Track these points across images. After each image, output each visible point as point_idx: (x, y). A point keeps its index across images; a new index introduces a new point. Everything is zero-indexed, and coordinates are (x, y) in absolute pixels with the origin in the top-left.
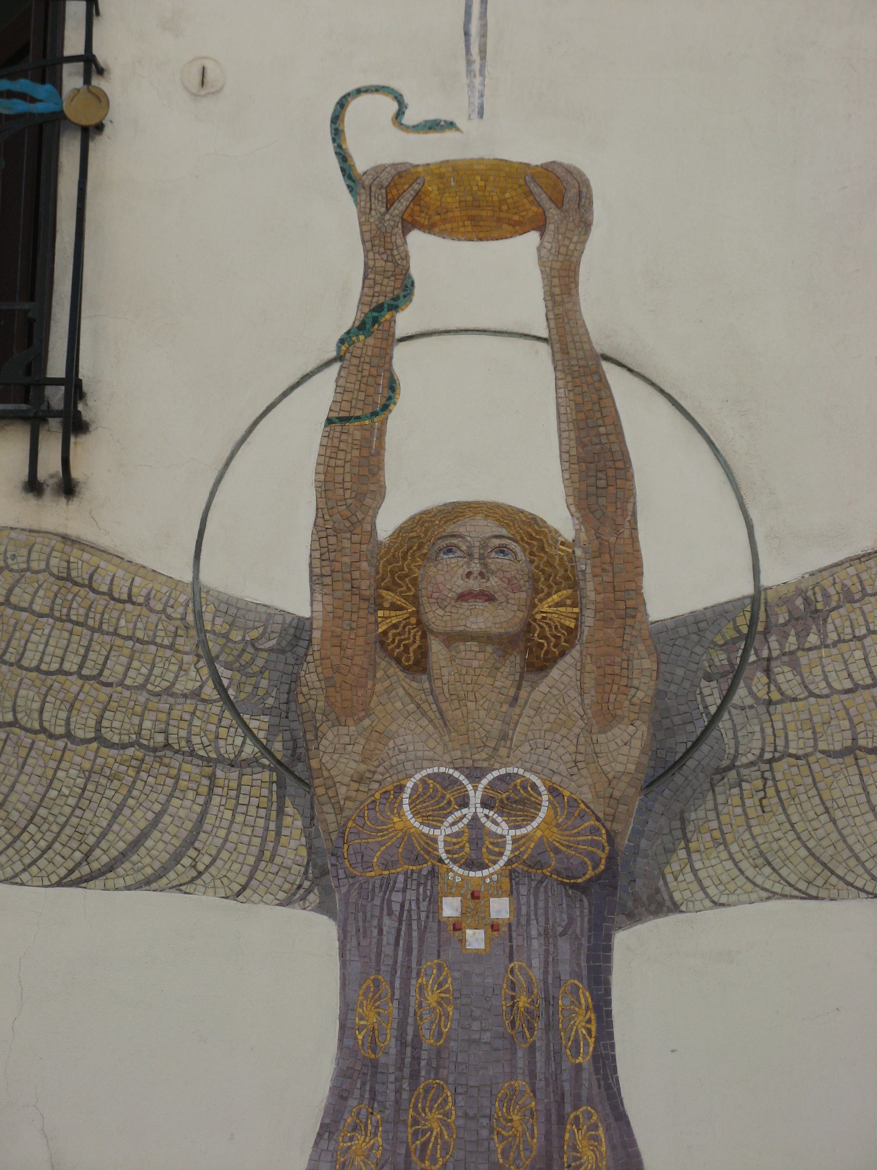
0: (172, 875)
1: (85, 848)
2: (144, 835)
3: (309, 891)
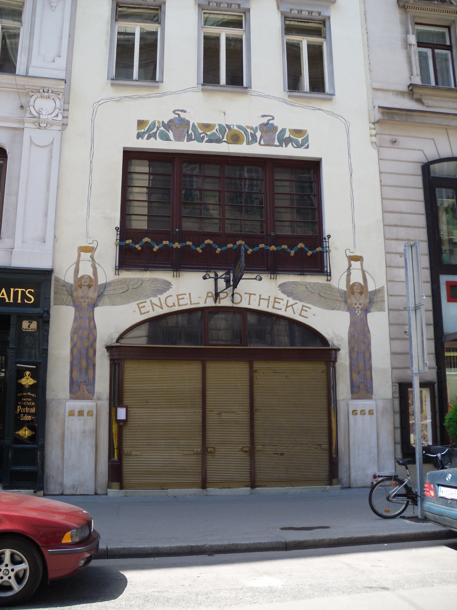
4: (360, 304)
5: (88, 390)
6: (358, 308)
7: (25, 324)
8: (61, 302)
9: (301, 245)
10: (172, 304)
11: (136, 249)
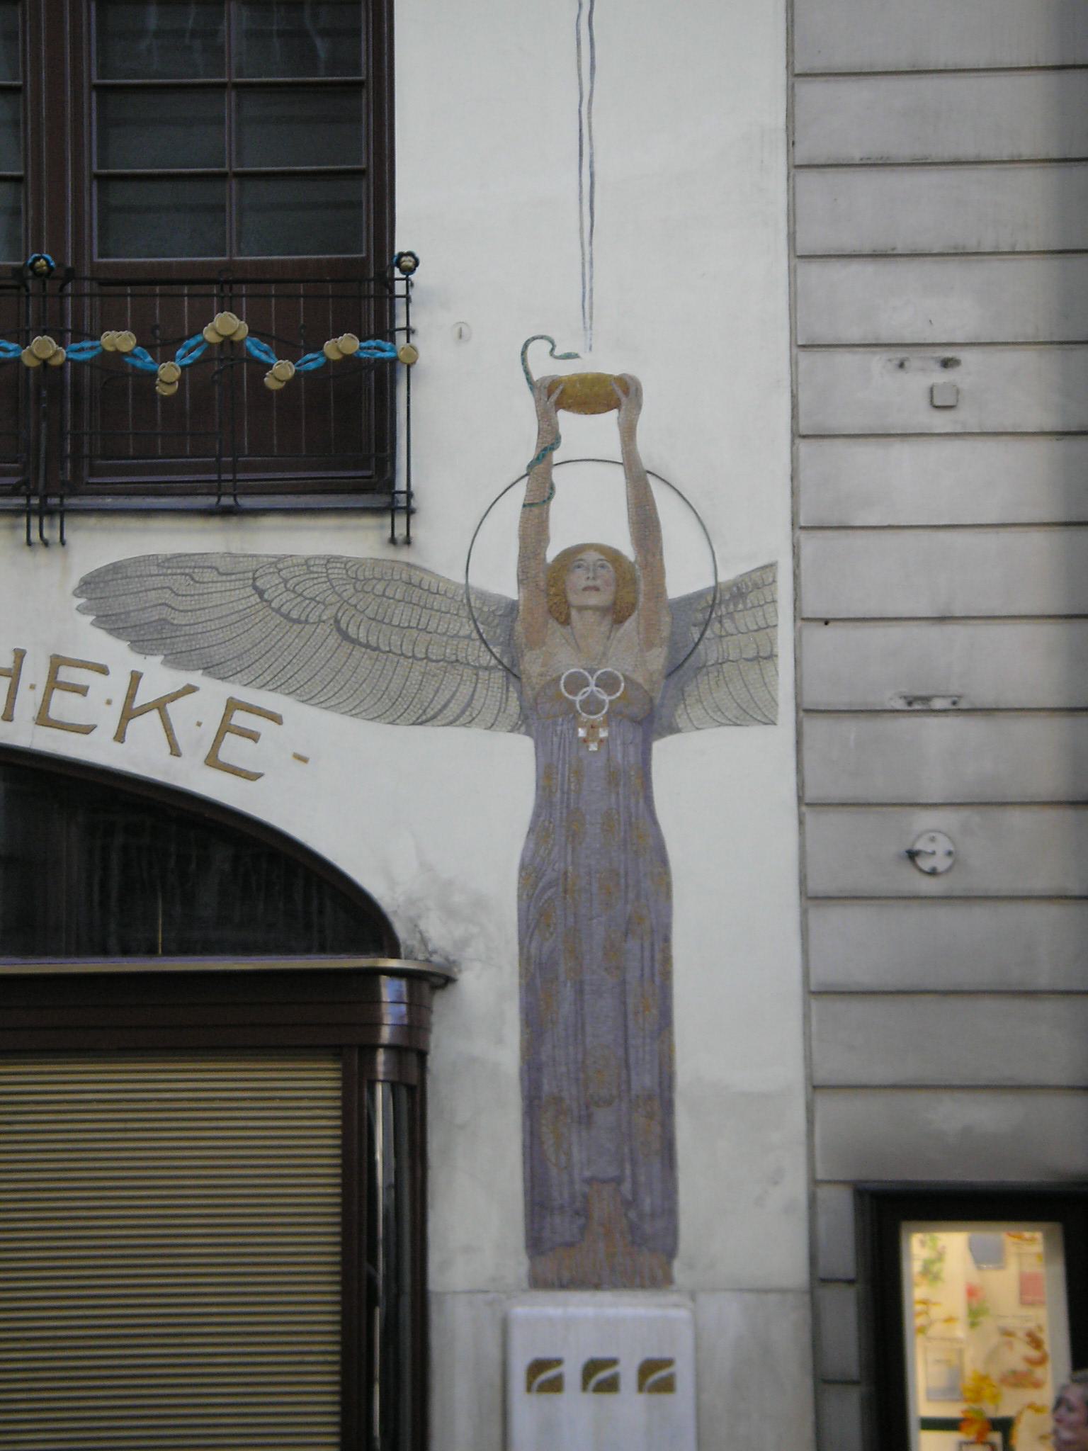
0: (461, 719)
1: (423, 708)
2: (449, 701)
3: (521, 725)
4: (608, 683)
6: (592, 705)
9: (226, 324)
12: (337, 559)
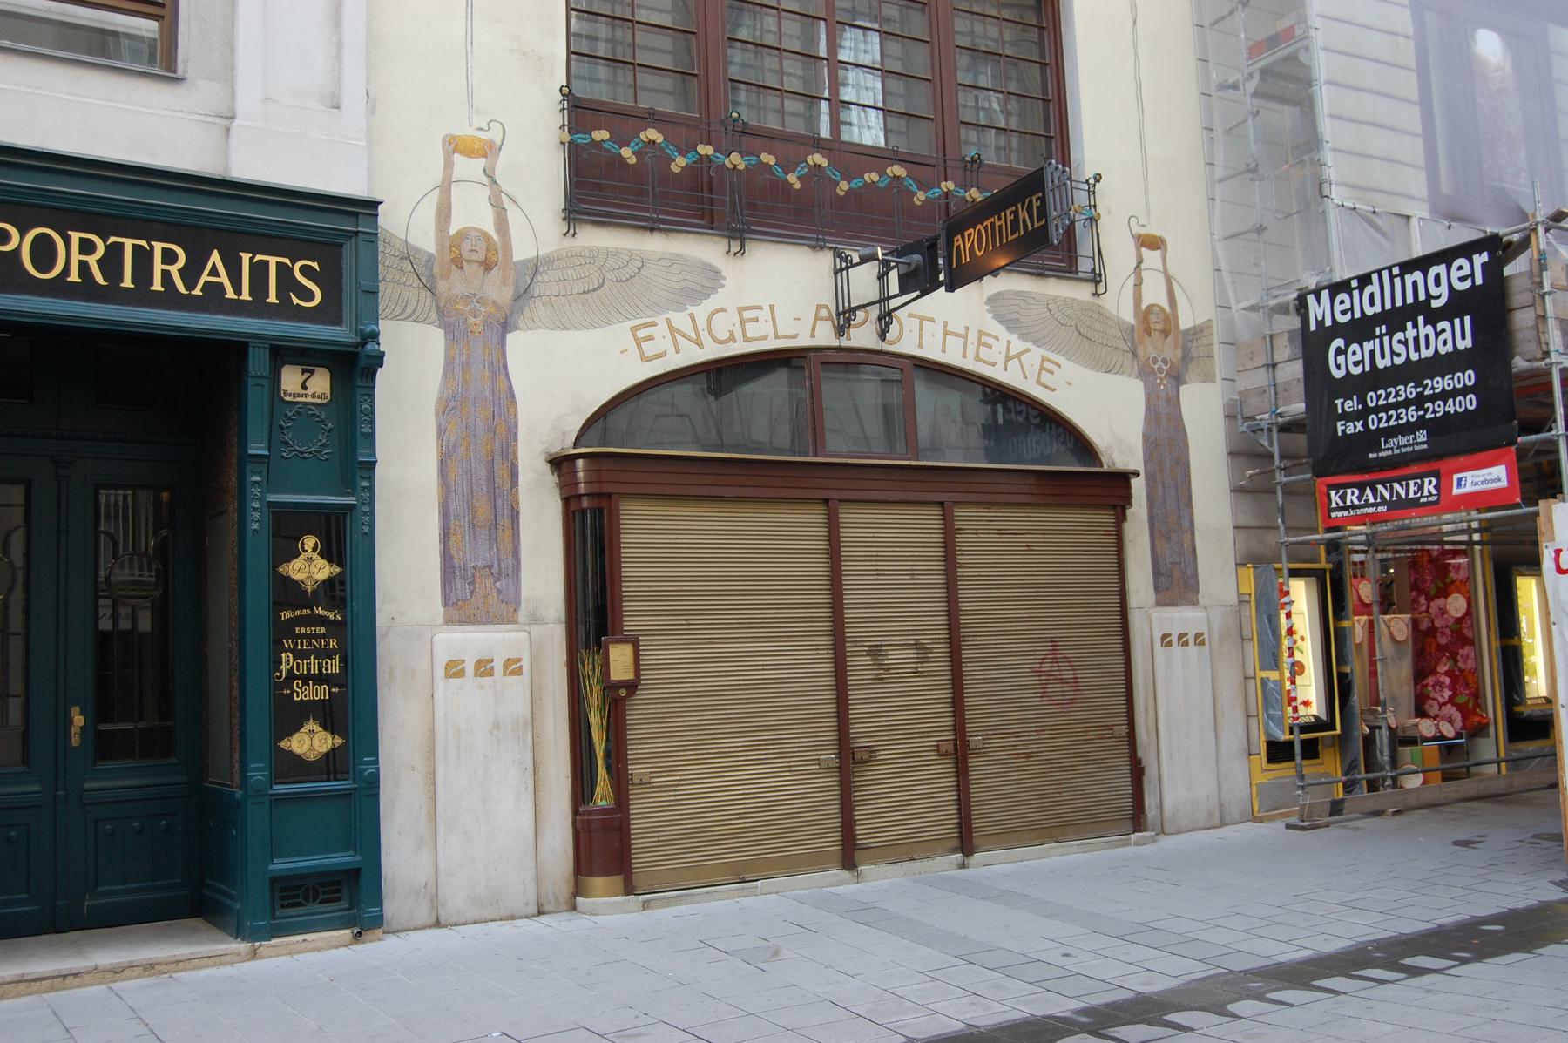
4: (1165, 361)
5: (499, 591)
7: (291, 379)
8: (398, 310)
10: (724, 336)
11: (623, 161)
12: (1075, 299)
